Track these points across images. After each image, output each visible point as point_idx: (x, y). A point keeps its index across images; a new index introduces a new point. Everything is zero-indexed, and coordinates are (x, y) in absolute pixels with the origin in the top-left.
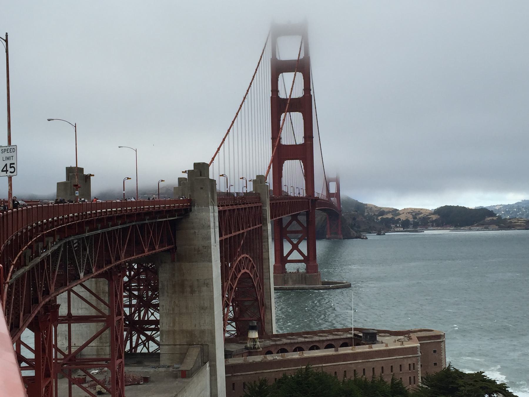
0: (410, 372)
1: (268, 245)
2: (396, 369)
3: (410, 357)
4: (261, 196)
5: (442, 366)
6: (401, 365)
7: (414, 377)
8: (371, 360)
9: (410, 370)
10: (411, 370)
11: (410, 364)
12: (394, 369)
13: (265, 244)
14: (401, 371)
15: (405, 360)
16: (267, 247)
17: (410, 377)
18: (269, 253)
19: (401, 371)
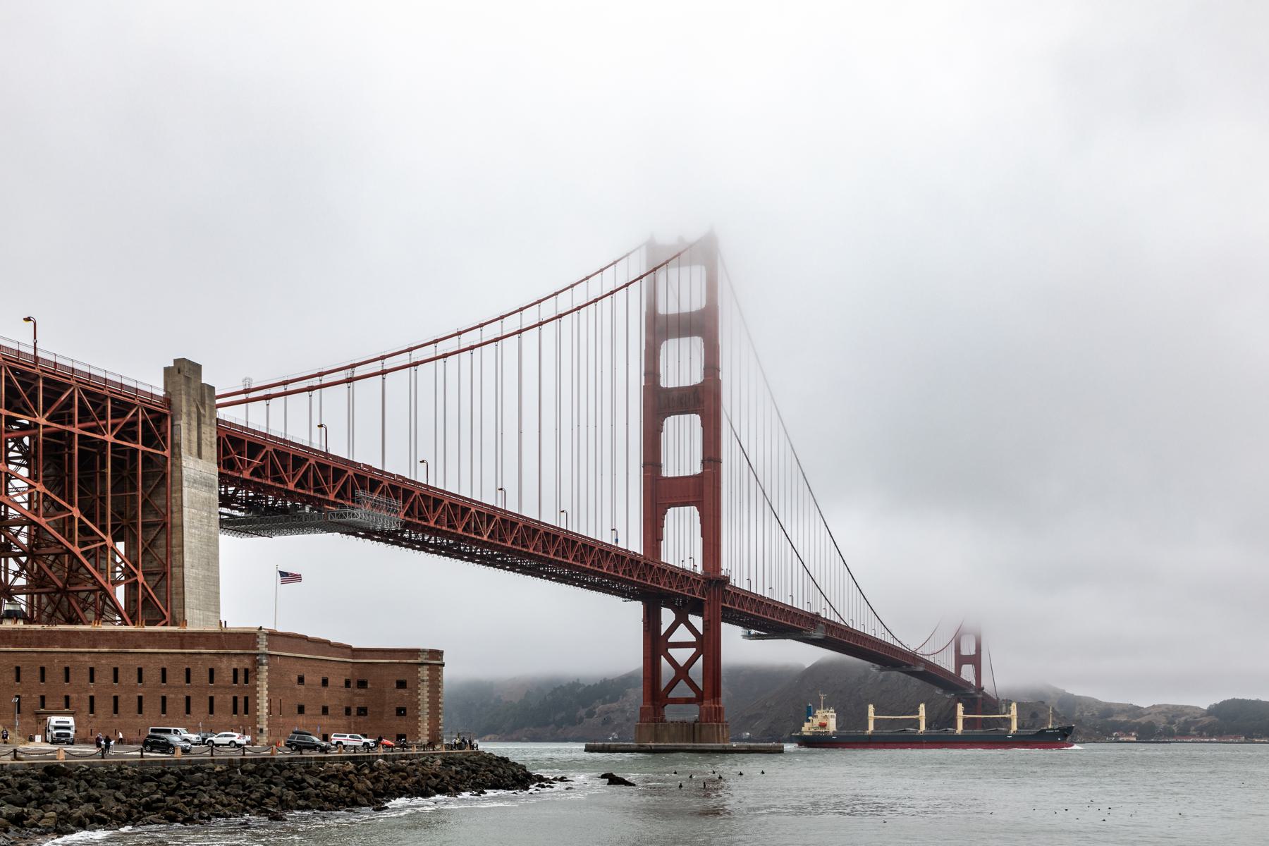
0: (235, 687)
1: (182, 497)
2: (200, 676)
3: (236, 654)
6: (211, 671)
7: (246, 699)
8: (131, 650)
9: (235, 681)
10: (239, 682)
11: (235, 671)
12: (192, 678)
13: (176, 495)
14: (211, 681)
15: (225, 659)
16: (180, 503)
17: (235, 699)
18: (182, 514)
19: (211, 681)
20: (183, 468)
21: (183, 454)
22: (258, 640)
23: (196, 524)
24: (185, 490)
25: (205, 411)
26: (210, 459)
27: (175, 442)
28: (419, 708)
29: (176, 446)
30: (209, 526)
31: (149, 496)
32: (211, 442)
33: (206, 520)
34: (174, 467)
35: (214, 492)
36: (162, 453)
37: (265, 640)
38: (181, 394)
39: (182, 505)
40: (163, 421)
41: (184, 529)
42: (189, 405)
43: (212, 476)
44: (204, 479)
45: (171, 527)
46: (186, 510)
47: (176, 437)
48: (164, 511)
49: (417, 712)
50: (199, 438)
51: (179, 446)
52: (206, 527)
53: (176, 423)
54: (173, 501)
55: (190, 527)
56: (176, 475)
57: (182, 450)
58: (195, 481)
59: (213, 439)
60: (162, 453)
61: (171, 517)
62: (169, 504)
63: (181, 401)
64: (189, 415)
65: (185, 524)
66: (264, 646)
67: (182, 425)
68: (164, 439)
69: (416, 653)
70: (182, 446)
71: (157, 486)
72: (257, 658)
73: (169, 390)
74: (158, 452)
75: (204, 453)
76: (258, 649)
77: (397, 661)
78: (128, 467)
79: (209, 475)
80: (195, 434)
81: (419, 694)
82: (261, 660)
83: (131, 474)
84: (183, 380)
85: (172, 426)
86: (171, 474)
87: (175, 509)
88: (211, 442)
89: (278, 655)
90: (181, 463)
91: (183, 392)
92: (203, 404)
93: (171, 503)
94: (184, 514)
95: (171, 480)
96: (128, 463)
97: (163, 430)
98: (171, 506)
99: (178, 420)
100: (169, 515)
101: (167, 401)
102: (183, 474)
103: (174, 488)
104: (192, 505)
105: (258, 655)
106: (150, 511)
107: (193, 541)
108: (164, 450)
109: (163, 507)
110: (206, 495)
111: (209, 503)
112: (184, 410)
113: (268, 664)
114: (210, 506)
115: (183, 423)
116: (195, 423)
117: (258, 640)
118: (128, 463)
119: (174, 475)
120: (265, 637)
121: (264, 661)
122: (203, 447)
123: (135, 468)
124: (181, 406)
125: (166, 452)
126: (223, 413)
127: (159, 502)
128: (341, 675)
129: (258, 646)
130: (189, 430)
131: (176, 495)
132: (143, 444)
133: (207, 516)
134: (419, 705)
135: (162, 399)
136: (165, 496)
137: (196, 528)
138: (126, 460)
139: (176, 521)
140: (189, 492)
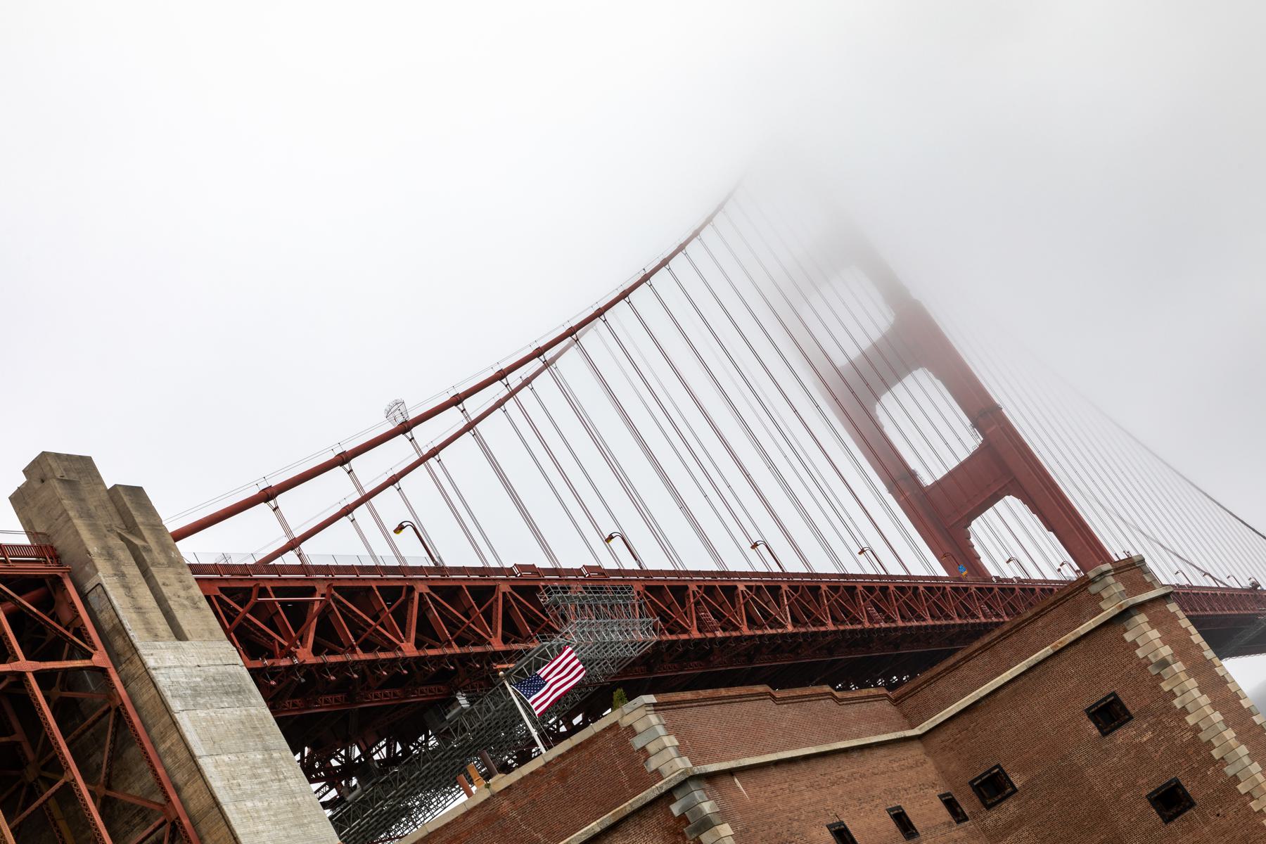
1: (182, 738)
4: (58, 543)
5: (1236, 779)
13: (168, 744)
16: (183, 755)
18: (202, 776)
20: (153, 672)
21: (138, 643)
22: (637, 743)
23: (247, 786)
24: (184, 720)
25: (144, 539)
26: (207, 635)
27: (107, 627)
28: (1216, 754)
29: (114, 635)
30: (280, 780)
31: (109, 787)
32: (189, 598)
33: (267, 771)
34: (132, 685)
35: (253, 701)
36: (87, 663)
37: (661, 730)
38: (70, 519)
39: (193, 757)
40: (58, 597)
41: (225, 808)
42: (100, 537)
43: (230, 669)
44: (214, 680)
45: (194, 825)
46: (207, 764)
47: (104, 617)
48: (159, 798)
49: (1219, 772)
50: (161, 601)
51: (120, 630)
52: (276, 785)
53: (89, 586)
54: (168, 761)
55: (237, 800)
56: (146, 697)
57: (131, 634)
58: (196, 692)
59: (191, 591)
60: (87, 663)
61: (183, 802)
62: (160, 771)
63: (77, 533)
64: (110, 555)
65: (222, 797)
66: (673, 752)
67: (104, 581)
68: (80, 632)
69: (1084, 595)
70: (128, 626)
71: (116, 755)
72: (676, 809)
73: (41, 528)
74: (78, 663)
75: (185, 626)
76: (658, 775)
77: (1047, 651)
78: (31, 756)
79: (221, 669)
80: (144, 592)
81: (1185, 711)
82: (693, 807)
83: (44, 768)
84: (60, 490)
85: (84, 598)
86: (134, 703)
87: (180, 777)
88: (189, 598)
89: (731, 772)
90: (144, 665)
91: (72, 514)
92: (132, 528)
93: (167, 771)
94: (207, 775)
95: (140, 716)
96: (27, 748)
97: (66, 616)
98: (170, 777)
99: (88, 577)
100: (173, 797)
101: (45, 548)
102: (160, 685)
103: (154, 731)
104: (217, 748)
105: (668, 796)
106: (127, 823)
107: (261, 827)
108: (89, 656)
109: (152, 792)
110: (238, 712)
111: (255, 728)
112: (94, 548)
113: (724, 816)
114: (260, 736)
115: (104, 574)
116: (133, 571)
117: (637, 743)
118: (27, 748)
119: (140, 702)
120: (653, 719)
121: (707, 807)
122: (179, 615)
123: (49, 745)
124: (82, 543)
125: (94, 658)
126: (195, 550)
127: (136, 789)
128: (922, 786)
129: (653, 764)
130: (127, 588)
131: (168, 744)
132: (29, 657)
133: (264, 760)
134: (1209, 744)
135: (34, 552)
136: (144, 765)
137: (252, 796)
138: (18, 743)
139: (197, 803)
140: (193, 722)
